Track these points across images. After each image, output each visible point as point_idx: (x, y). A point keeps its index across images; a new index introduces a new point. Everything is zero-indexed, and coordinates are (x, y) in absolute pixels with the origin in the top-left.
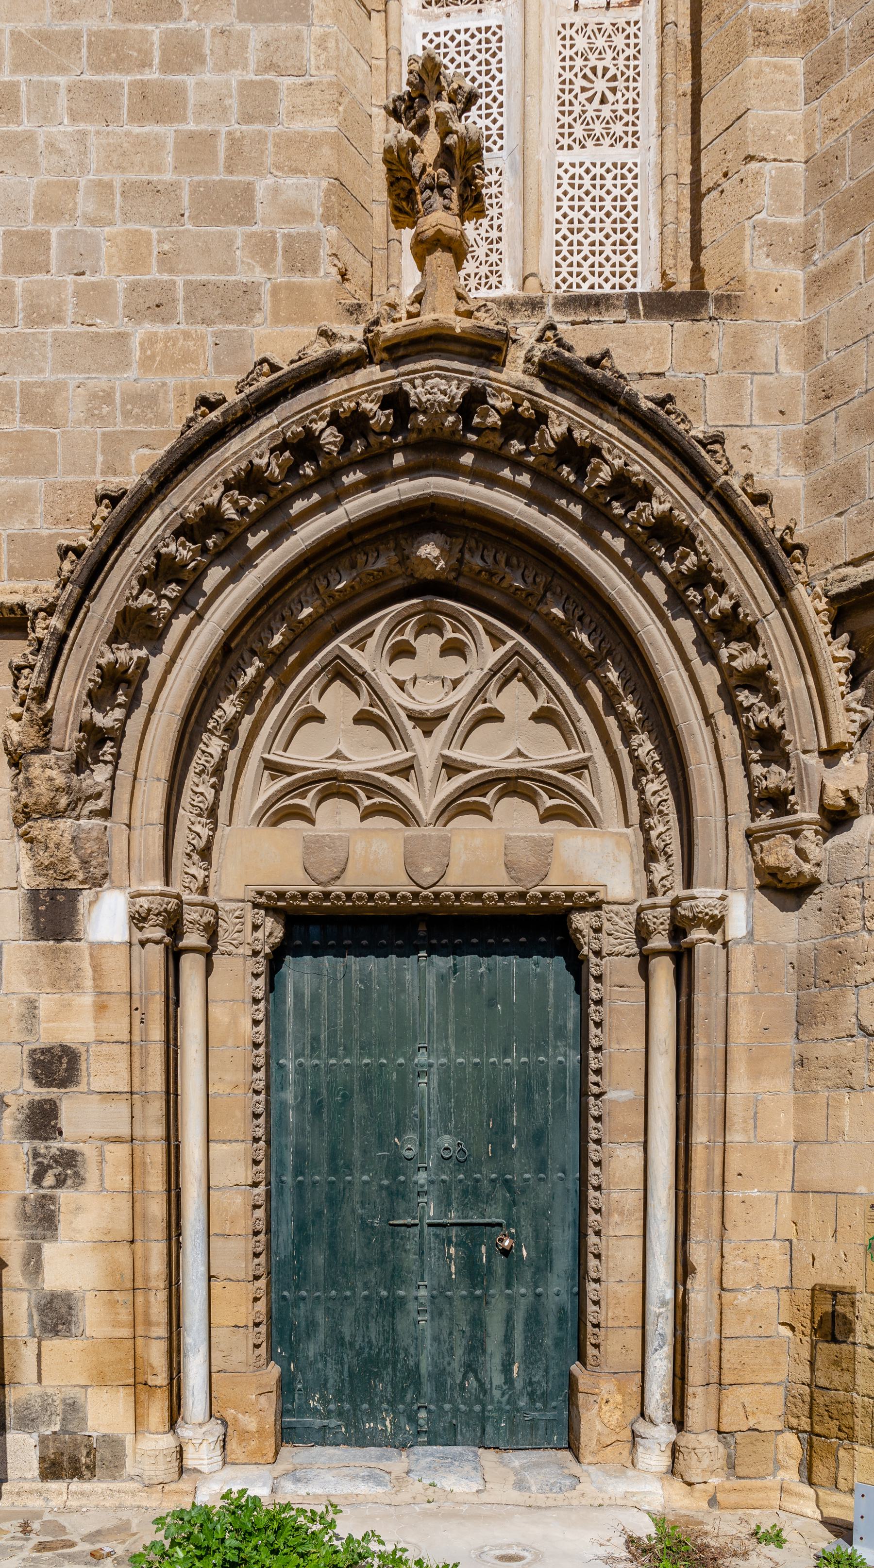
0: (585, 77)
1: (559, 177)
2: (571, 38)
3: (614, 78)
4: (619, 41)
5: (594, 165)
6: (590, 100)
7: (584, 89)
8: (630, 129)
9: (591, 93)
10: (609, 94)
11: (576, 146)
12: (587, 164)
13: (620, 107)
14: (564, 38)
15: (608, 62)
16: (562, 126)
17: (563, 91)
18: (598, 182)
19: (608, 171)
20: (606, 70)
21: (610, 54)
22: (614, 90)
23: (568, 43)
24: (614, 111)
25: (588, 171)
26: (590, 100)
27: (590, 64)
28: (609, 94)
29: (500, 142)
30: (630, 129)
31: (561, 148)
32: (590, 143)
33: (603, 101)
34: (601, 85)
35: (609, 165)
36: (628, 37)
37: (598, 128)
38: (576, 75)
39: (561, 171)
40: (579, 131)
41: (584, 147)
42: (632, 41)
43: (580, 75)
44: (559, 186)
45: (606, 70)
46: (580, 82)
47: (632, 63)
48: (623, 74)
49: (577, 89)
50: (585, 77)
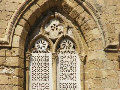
0: (65, 66)
1: (61, 86)
2: (63, 59)
3: (71, 67)
4: (72, 60)
5: (68, 84)
6: (66, 71)
7: (65, 69)
8: (74, 77)
9: (67, 70)
10: (70, 70)
11: (64, 80)
12: (66, 83)
13: (72, 73)
14: (61, 59)
15: (70, 64)
16: (61, 76)
17: (61, 69)
18: (68, 87)
19: (70, 85)
20: (69, 65)
21: (70, 62)
22: (71, 69)
23: (62, 60)
24: (71, 73)
25: (66, 85)
26: (66, 71)
27: (66, 64)
28: (70, 70)
29: (48, 79)
30: (74, 77)
31: (61, 80)
32: (66, 79)
33: (69, 71)
34: (68, 68)
35: (71, 84)
36: (74, 59)
37: (68, 76)
38: (63, 66)
39: (61, 85)
40: (64, 77)
41: (65, 80)
42: (75, 60)
43: (64, 66)
44: (61, 88)
45: (69, 65)
46: (64, 67)
47: (75, 64)
48: (73, 66)
49: (64, 69)
50: (65, 66)
